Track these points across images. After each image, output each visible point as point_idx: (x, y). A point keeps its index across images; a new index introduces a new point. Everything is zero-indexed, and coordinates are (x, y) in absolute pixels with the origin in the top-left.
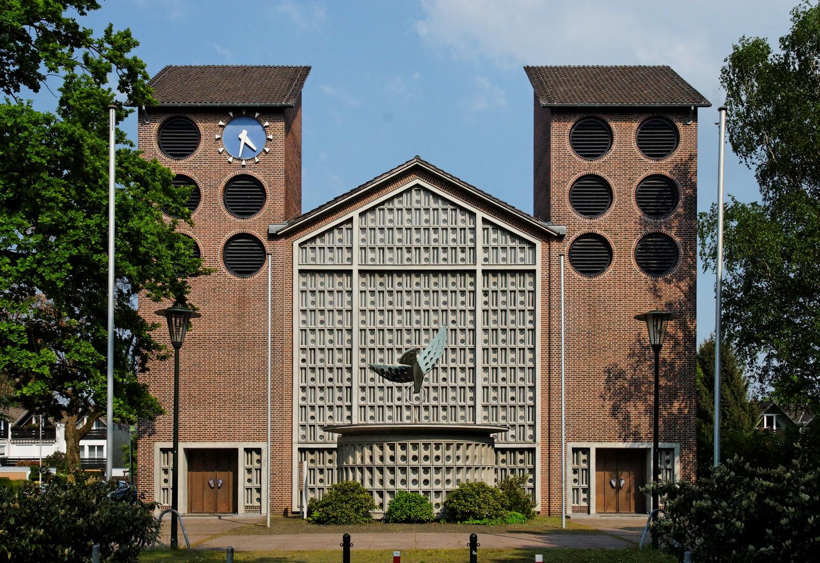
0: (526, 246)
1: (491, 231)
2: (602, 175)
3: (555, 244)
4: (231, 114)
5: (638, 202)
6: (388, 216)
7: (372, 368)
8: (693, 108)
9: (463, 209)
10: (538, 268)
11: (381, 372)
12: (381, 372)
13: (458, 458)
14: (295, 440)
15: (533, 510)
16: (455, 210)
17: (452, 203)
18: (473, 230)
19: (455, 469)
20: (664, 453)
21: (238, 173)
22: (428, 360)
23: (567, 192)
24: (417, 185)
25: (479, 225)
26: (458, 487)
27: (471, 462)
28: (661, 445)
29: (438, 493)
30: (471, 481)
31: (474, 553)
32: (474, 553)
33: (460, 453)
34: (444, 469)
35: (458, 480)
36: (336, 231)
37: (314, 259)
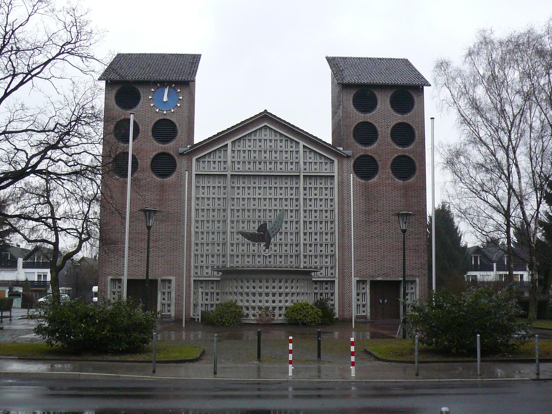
0: (329, 161)
1: (308, 153)
2: (371, 122)
3: (345, 162)
4: (159, 85)
5: (393, 140)
6: (248, 143)
7: (238, 233)
8: (421, 87)
9: (292, 140)
10: (336, 174)
11: (244, 235)
12: (244, 235)
13: (292, 287)
14: (192, 274)
15: (335, 317)
16: (287, 140)
17: (286, 136)
18: (297, 152)
19: (290, 294)
20: (409, 284)
21: (161, 118)
22: (273, 229)
23: (352, 131)
24: (265, 126)
25: (301, 149)
26: (292, 304)
27: (299, 290)
28: (407, 279)
29: (280, 308)
30: (300, 302)
31: (319, 339)
32: (319, 339)
33: (293, 284)
34: (284, 294)
35: (292, 301)
36: (217, 152)
37: (204, 168)
